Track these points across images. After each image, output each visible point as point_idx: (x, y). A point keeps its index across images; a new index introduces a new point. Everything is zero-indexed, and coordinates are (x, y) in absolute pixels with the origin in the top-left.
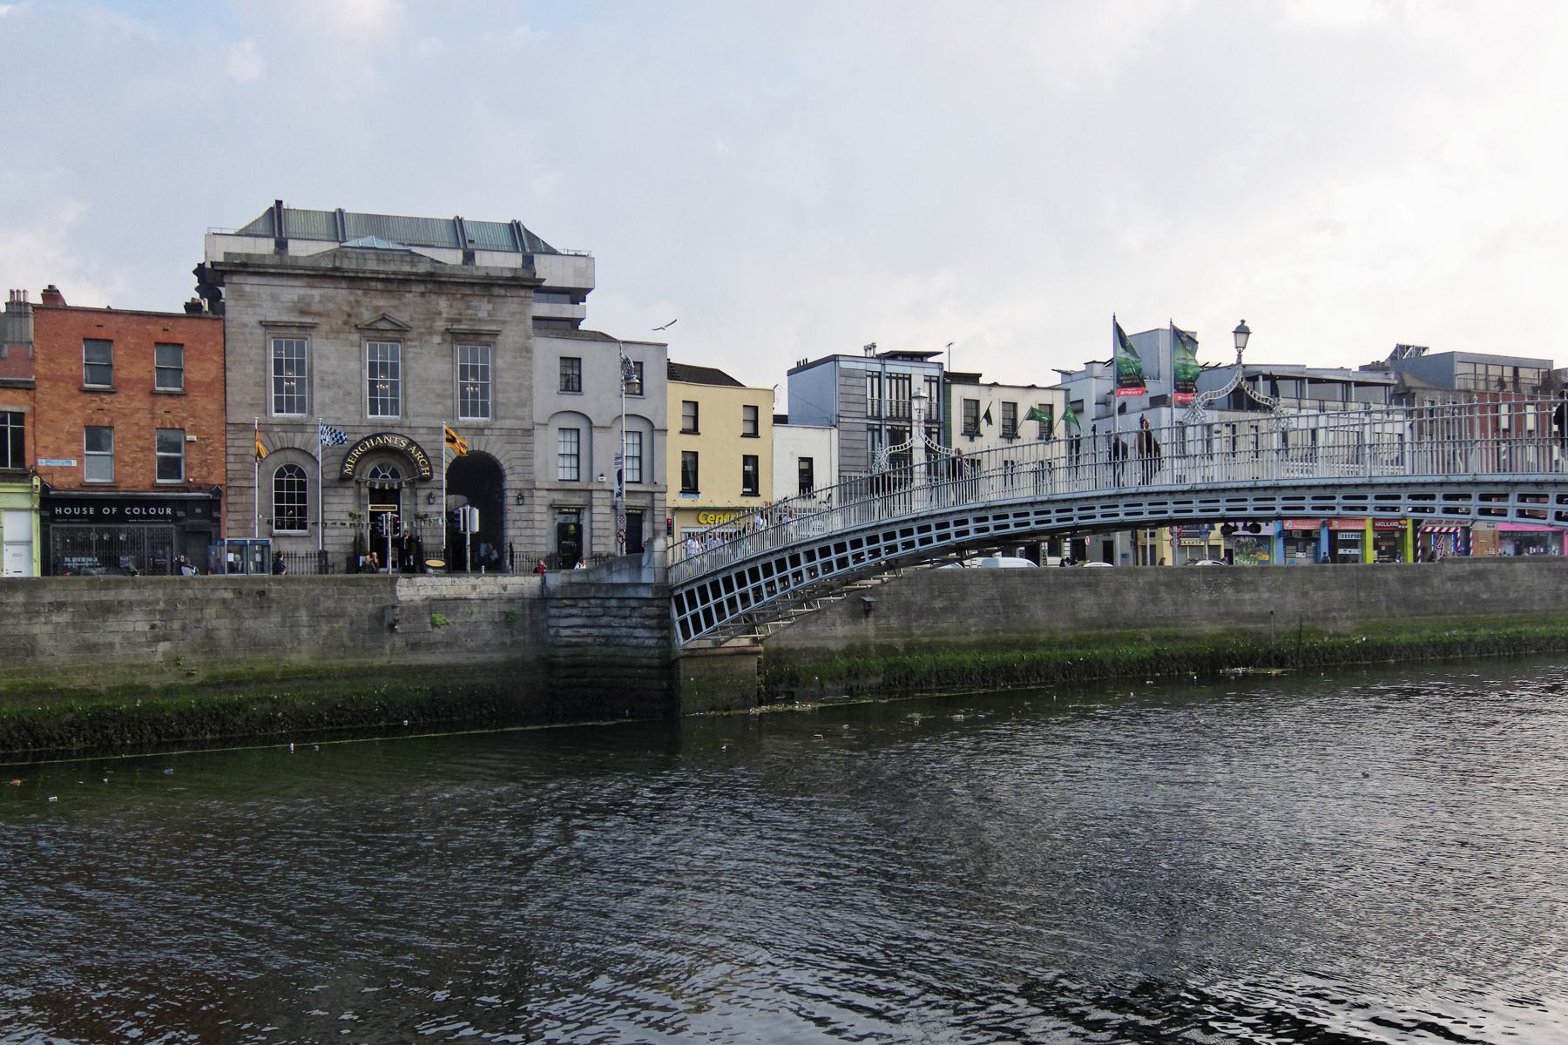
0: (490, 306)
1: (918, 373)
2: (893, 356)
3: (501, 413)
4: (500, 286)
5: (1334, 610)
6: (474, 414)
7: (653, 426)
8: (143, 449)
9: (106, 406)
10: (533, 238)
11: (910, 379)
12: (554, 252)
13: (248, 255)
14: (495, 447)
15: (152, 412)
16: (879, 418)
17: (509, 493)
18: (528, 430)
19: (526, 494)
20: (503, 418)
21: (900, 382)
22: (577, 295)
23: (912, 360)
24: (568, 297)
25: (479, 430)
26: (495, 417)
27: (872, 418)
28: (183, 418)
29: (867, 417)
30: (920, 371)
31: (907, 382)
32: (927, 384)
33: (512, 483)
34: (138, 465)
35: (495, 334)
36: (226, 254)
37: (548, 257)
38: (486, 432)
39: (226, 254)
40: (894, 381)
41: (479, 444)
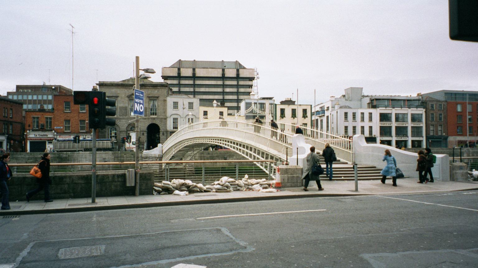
0: (156, 91)
1: (267, 102)
2: (264, 99)
3: (159, 115)
4: (159, 86)
5: (319, 162)
6: (153, 115)
7: (196, 117)
8: (77, 124)
9: (68, 115)
10: (240, 64)
11: (265, 104)
12: (244, 68)
13: (104, 82)
14: (157, 122)
15: (79, 116)
16: (257, 114)
17: (161, 133)
18: (165, 118)
19: (165, 133)
20: (160, 116)
21: (263, 105)
22: (251, 79)
23: (267, 99)
24: (248, 79)
25: (154, 119)
26: (158, 116)
27: (255, 113)
28: (85, 118)
29: (253, 114)
30: (267, 102)
31: (264, 105)
32: (270, 105)
33: (162, 129)
34: (76, 128)
35: (158, 97)
36: (99, 82)
37: (244, 70)
38: (156, 119)
39: (99, 82)
40: (261, 105)
41: (154, 122)
